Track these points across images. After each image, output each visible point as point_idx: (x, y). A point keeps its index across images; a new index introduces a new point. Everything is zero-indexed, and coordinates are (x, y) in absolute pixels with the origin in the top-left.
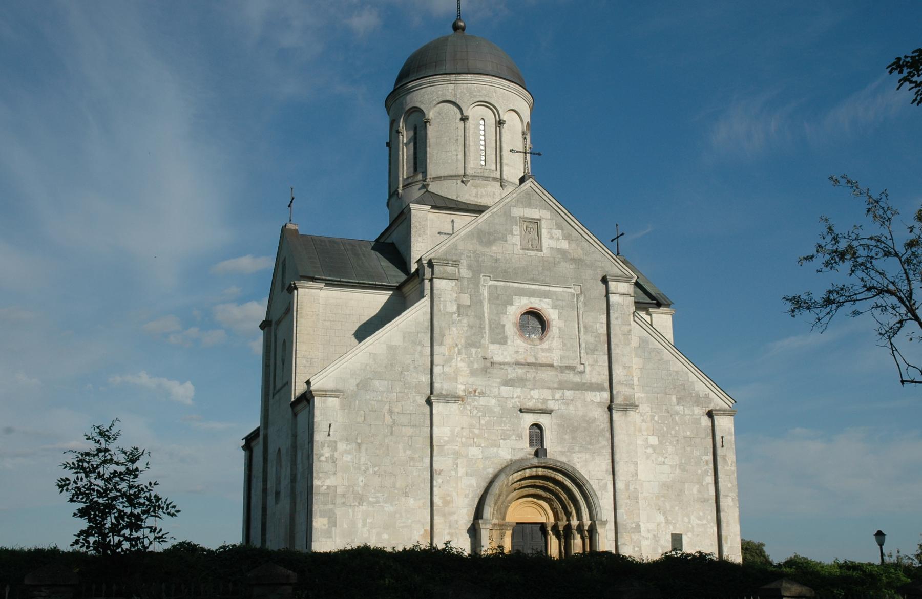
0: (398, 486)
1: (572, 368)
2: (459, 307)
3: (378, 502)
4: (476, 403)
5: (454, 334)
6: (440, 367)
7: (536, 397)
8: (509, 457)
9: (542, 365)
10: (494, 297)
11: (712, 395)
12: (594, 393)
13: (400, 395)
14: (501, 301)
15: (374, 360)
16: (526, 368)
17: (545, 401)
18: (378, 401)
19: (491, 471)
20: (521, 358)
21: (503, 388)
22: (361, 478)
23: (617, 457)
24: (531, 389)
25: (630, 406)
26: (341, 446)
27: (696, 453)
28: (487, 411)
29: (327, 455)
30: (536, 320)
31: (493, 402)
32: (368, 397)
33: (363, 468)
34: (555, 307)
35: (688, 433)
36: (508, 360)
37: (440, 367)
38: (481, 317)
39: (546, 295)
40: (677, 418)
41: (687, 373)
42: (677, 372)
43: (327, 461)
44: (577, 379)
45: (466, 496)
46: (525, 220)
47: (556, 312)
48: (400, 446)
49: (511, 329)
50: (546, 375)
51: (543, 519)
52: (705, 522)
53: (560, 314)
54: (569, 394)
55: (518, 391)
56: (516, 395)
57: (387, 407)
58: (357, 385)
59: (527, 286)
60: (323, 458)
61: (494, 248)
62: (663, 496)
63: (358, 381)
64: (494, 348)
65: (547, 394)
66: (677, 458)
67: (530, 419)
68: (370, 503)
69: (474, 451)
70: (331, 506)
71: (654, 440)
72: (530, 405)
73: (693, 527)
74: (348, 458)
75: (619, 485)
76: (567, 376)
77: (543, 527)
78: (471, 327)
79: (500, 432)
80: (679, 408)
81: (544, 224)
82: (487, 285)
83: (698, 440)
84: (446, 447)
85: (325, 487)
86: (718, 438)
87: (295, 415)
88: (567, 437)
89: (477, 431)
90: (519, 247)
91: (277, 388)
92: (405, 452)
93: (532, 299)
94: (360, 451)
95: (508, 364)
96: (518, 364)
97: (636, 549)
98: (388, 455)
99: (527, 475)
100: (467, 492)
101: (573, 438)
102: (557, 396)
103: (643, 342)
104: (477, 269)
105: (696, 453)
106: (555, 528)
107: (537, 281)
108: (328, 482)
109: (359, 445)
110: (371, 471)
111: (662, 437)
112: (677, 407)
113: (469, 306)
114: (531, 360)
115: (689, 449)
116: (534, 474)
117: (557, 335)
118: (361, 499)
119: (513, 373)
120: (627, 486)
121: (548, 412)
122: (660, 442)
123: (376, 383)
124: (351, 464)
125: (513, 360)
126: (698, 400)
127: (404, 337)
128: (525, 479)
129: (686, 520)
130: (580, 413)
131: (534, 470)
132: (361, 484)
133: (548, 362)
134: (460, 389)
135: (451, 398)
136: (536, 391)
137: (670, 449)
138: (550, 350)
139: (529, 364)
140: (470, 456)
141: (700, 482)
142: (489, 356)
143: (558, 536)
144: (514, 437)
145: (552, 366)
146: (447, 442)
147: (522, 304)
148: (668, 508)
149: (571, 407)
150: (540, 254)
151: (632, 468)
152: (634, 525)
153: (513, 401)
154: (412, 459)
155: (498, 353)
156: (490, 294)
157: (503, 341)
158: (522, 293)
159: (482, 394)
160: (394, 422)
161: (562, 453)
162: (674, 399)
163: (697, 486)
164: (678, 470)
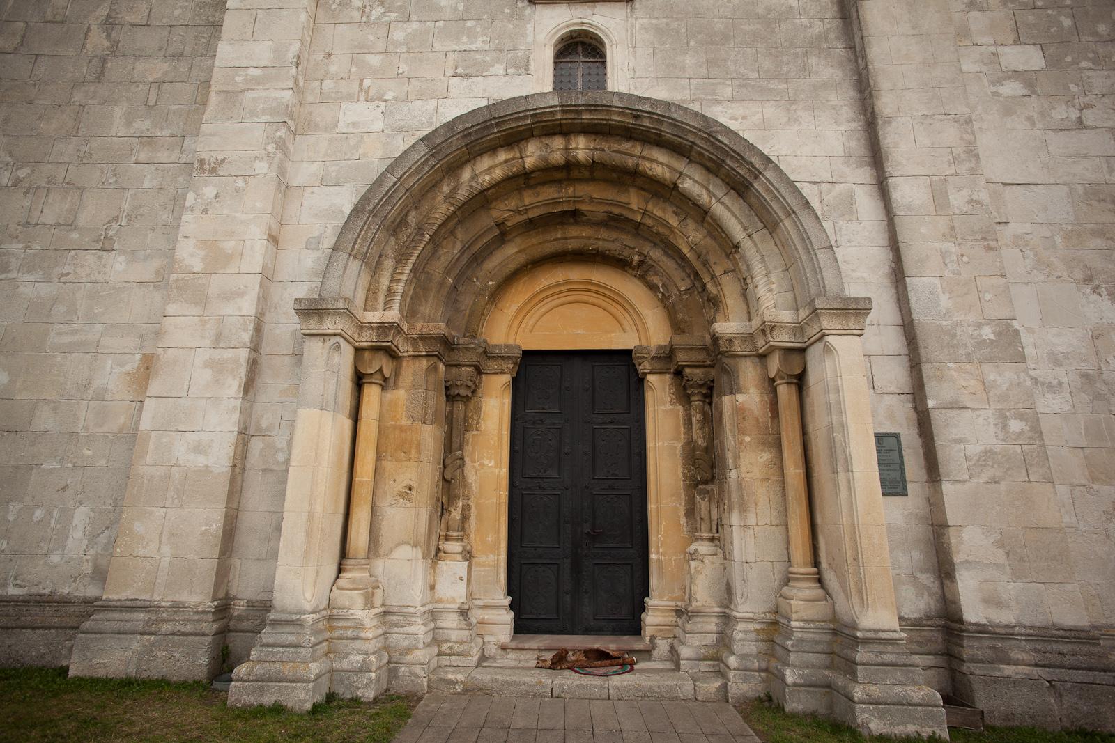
0: (83, 219)
23: (886, 103)
69: (359, 116)
75: (906, 192)
84: (249, 95)
88: (689, 60)
89: (374, 60)
92: (129, 123)
97: (1015, 426)
99: (530, 162)
100: (315, 231)
101: (710, 63)
116: (557, 157)
128: (523, 180)
131: (558, 143)
140: (342, 127)
143: (683, 391)
144: (499, 69)
146: (258, 81)
152: (988, 333)
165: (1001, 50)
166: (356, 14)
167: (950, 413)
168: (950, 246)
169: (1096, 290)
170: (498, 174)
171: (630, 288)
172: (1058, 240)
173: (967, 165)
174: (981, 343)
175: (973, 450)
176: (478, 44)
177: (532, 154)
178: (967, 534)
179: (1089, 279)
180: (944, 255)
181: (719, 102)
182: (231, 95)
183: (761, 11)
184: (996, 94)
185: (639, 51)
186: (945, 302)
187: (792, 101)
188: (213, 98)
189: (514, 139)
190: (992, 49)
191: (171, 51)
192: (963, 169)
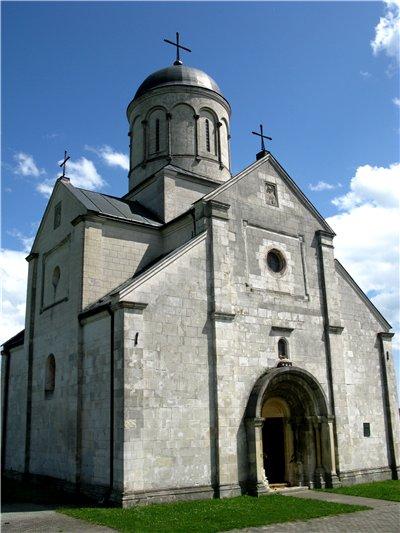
3: (174, 404)
5: (226, 263)
8: (266, 365)
10: (251, 237)
15: (169, 279)
17: (287, 322)
18: (173, 315)
19: (255, 377)
20: (270, 287)
22: (161, 383)
24: (279, 312)
25: (338, 330)
26: (146, 354)
28: (249, 327)
30: (276, 261)
31: (254, 320)
45: (238, 398)
46: (267, 184)
49: (262, 264)
50: (287, 301)
51: (281, 415)
54: (301, 316)
60: (131, 365)
64: (252, 276)
65: (288, 315)
68: (170, 406)
69: (243, 361)
70: (139, 409)
71: (351, 354)
74: (150, 364)
75: (335, 388)
77: (279, 420)
81: (279, 188)
82: (245, 230)
87: (82, 326)
89: (244, 344)
91: (46, 305)
96: (268, 291)
102: (295, 318)
104: (239, 215)
106: (292, 422)
108: (137, 386)
111: (355, 351)
114: (276, 289)
118: (161, 400)
121: (290, 330)
123: (171, 299)
132: (161, 388)
133: (287, 291)
135: (228, 317)
143: (293, 429)
146: (226, 352)
154: (200, 366)
155: (257, 283)
157: (258, 272)
158: (268, 238)
159: (247, 314)
161: (301, 362)
171: (283, 403)
182: (222, 356)
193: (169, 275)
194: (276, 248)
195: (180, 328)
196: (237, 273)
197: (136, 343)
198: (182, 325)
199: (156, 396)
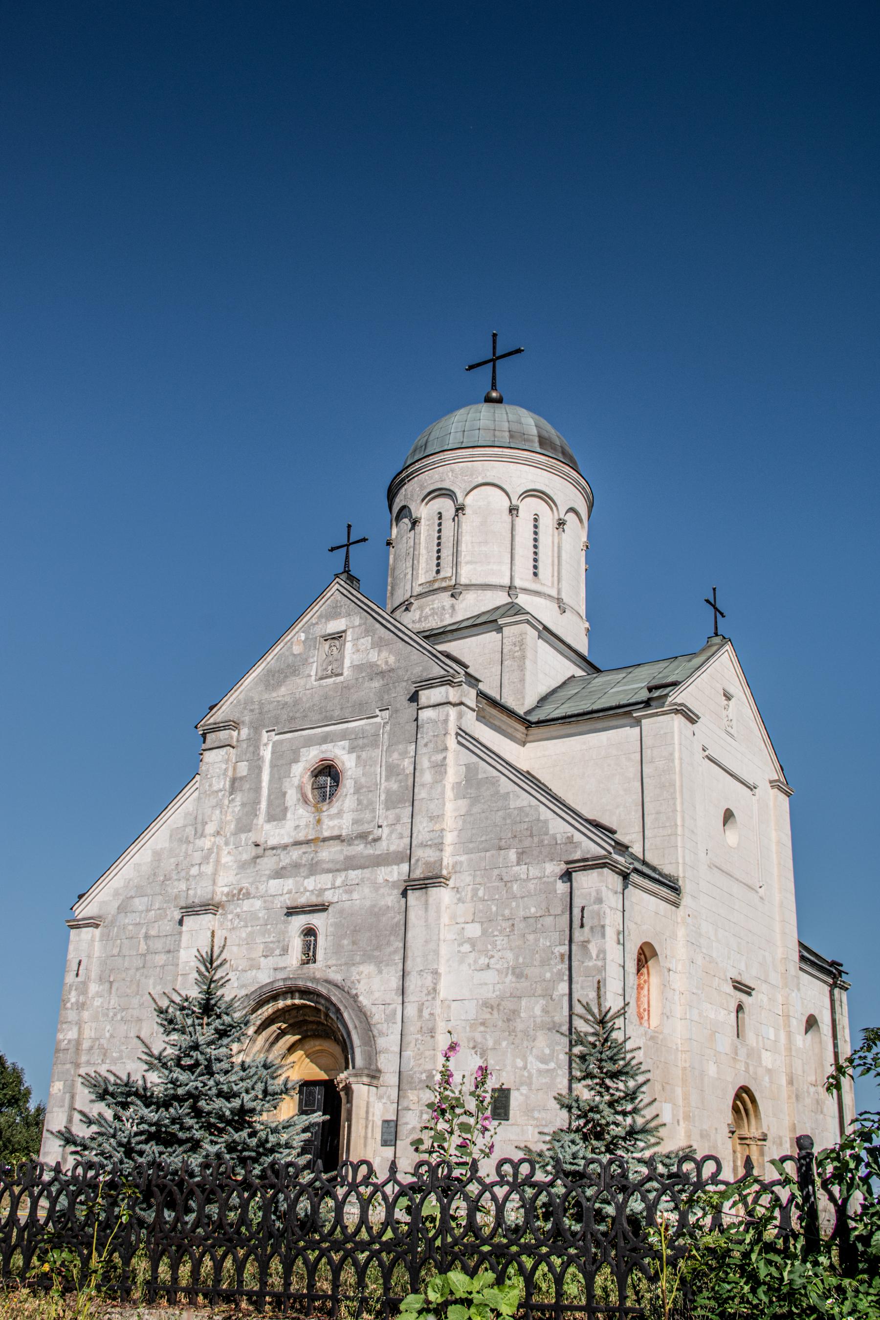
1: (363, 836)
2: (234, 780)
3: (121, 1058)
4: (238, 910)
6: (197, 867)
7: (311, 888)
9: (324, 840)
11: (578, 837)
12: (389, 869)
13: (158, 912)
14: (284, 760)
16: (304, 848)
17: (322, 891)
20: (301, 837)
21: (272, 882)
22: (108, 1027)
23: (409, 963)
27: (544, 942)
28: (254, 916)
29: (73, 1000)
30: (327, 774)
31: (258, 904)
32: (127, 921)
33: (111, 1014)
34: (352, 750)
35: (533, 910)
36: (286, 840)
37: (197, 867)
38: (258, 789)
39: (343, 736)
40: (515, 887)
41: (536, 809)
42: (521, 809)
43: (72, 1009)
44: (370, 851)
47: (354, 755)
48: (151, 981)
49: (292, 796)
50: (328, 853)
52: (552, 1065)
53: (358, 757)
54: (353, 875)
55: (289, 883)
56: (286, 891)
57: (144, 931)
58: (118, 909)
59: (319, 730)
61: (283, 690)
62: (483, 1024)
63: (120, 902)
64: (267, 827)
65: (324, 880)
66: (510, 955)
67: (299, 922)
71: (474, 930)
72: (302, 900)
73: (530, 1076)
76: (360, 850)
78: (243, 805)
79: (262, 946)
80: (521, 870)
83: (549, 920)
85: (66, 1042)
86: (576, 912)
88: (345, 942)
90: (313, 678)
93: (324, 747)
94: (110, 993)
95: (285, 847)
96: (297, 843)
98: (137, 994)
101: (354, 943)
102: (338, 882)
103: (470, 770)
105: (544, 942)
107: (332, 718)
109: (111, 983)
110: (119, 1017)
111: (487, 920)
112: (518, 868)
113: (245, 776)
115: (531, 937)
117: (352, 791)
119: (286, 859)
120: (420, 1011)
122: (484, 932)
123: (137, 901)
124: (100, 1009)
125: (291, 840)
126: (551, 851)
127: (171, 836)
129: (520, 1063)
130: (368, 903)
132: (108, 1035)
133: (336, 833)
134: (221, 891)
136: (312, 878)
137: (501, 941)
138: (340, 814)
139: (308, 842)
141: (548, 995)
142: (261, 841)
144: (277, 952)
145: (338, 838)
147: (312, 756)
148: (490, 1043)
149: (355, 896)
150: (340, 679)
151: (429, 979)
152: (424, 1077)
153: (282, 899)
156: (273, 753)
159: (248, 895)
160: (148, 950)
162: (512, 855)
163: (542, 1002)
164: (510, 977)
165: (467, 926)
166: (229, 923)
167: (405, 1112)
168: (419, 1036)
169: (476, 1053)
170: (270, 1011)
172: (468, 1028)
173: (433, 995)
174: (421, 1081)
175: (410, 1126)
176: (272, 939)
177: (281, 1004)
178: (401, 1161)
179: (474, 1048)
180: (417, 1040)
181: (354, 965)
183: (376, 910)
184: (459, 952)
185: (329, 938)
186: (412, 1063)
187: (381, 962)
188: (180, 978)
189: (275, 997)
190: (463, 925)
191: (167, 949)
192: (430, 998)
193: (138, 865)
194: (329, 755)
195: (142, 942)
196: (244, 826)
197: (77, 975)
198: (147, 937)
199: (101, 1047)
